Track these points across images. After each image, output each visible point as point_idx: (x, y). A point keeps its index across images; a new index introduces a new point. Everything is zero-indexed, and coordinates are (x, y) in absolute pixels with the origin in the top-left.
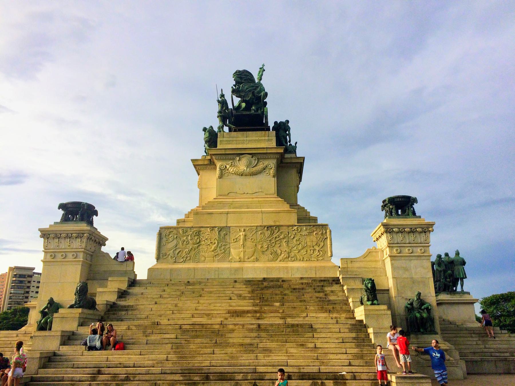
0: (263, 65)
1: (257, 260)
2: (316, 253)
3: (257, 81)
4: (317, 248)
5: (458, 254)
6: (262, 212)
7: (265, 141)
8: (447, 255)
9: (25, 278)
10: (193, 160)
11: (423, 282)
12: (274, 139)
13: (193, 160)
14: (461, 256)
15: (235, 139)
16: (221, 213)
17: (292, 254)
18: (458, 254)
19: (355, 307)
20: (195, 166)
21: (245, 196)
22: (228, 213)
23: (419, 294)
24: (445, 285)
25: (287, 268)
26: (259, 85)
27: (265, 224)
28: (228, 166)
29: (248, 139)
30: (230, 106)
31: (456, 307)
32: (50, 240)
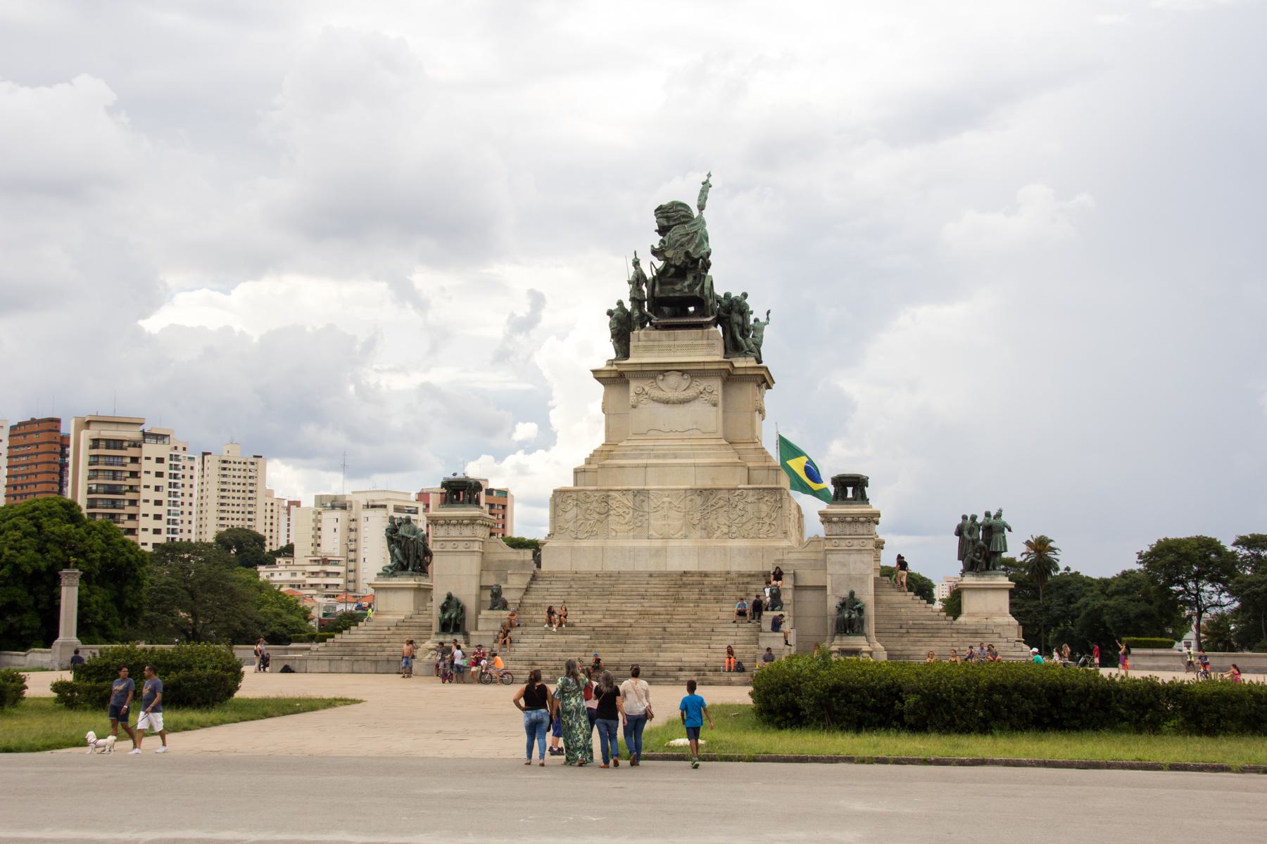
0: (709, 175)
1: (686, 537)
2: (766, 527)
3: (696, 213)
4: (767, 520)
6: (695, 465)
7: (703, 347)
9: (122, 448)
10: (594, 372)
11: (862, 580)
13: (594, 372)
16: (637, 466)
17: (734, 529)
21: (671, 436)
22: (646, 466)
23: (852, 594)
24: (973, 562)
25: (724, 548)
27: (700, 485)
28: (647, 389)
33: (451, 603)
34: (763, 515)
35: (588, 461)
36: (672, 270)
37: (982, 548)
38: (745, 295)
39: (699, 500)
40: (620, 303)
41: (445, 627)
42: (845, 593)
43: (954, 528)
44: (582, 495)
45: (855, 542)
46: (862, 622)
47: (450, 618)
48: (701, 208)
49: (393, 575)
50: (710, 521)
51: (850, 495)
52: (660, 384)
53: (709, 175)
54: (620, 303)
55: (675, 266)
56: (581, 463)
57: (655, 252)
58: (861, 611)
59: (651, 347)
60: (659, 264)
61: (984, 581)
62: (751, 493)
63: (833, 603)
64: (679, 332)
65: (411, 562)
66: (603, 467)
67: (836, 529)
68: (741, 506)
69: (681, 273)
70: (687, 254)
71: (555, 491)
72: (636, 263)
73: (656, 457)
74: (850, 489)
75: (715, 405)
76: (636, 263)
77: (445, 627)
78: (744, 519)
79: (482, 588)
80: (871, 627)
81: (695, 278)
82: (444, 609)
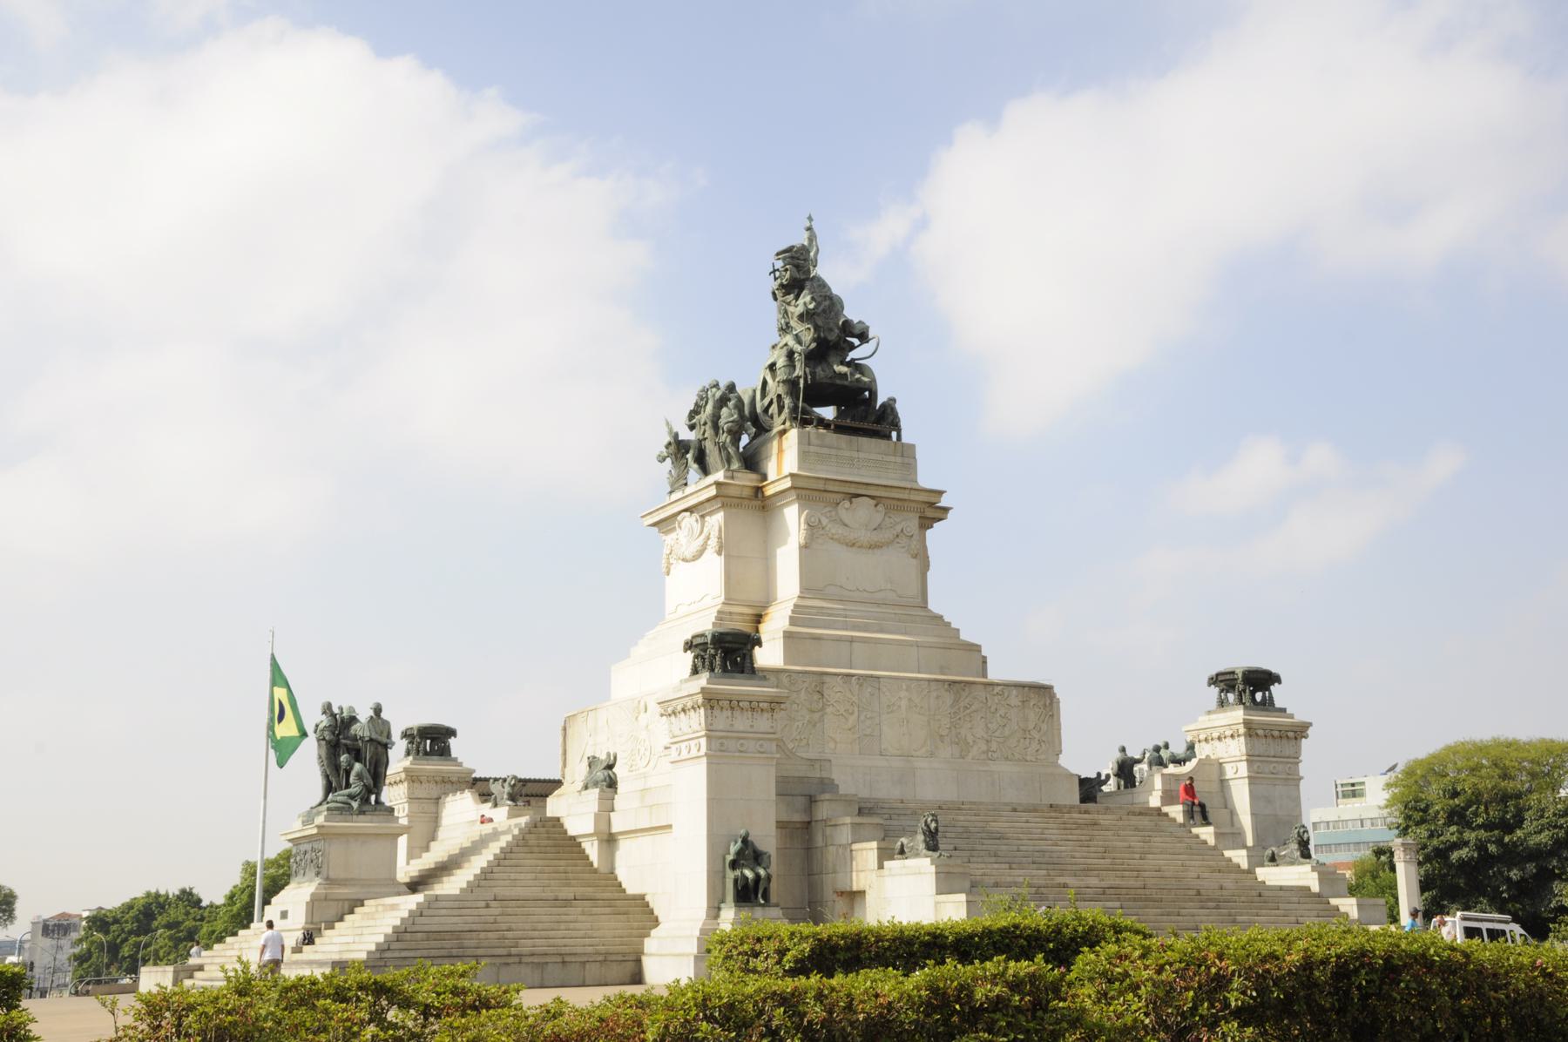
1: (932, 755)
2: (1035, 746)
15: (833, 452)
16: (839, 639)
17: (994, 746)
22: (852, 640)
28: (825, 521)
29: (862, 455)
32: (717, 712)
39: (948, 698)
64: (864, 441)
68: (1002, 712)
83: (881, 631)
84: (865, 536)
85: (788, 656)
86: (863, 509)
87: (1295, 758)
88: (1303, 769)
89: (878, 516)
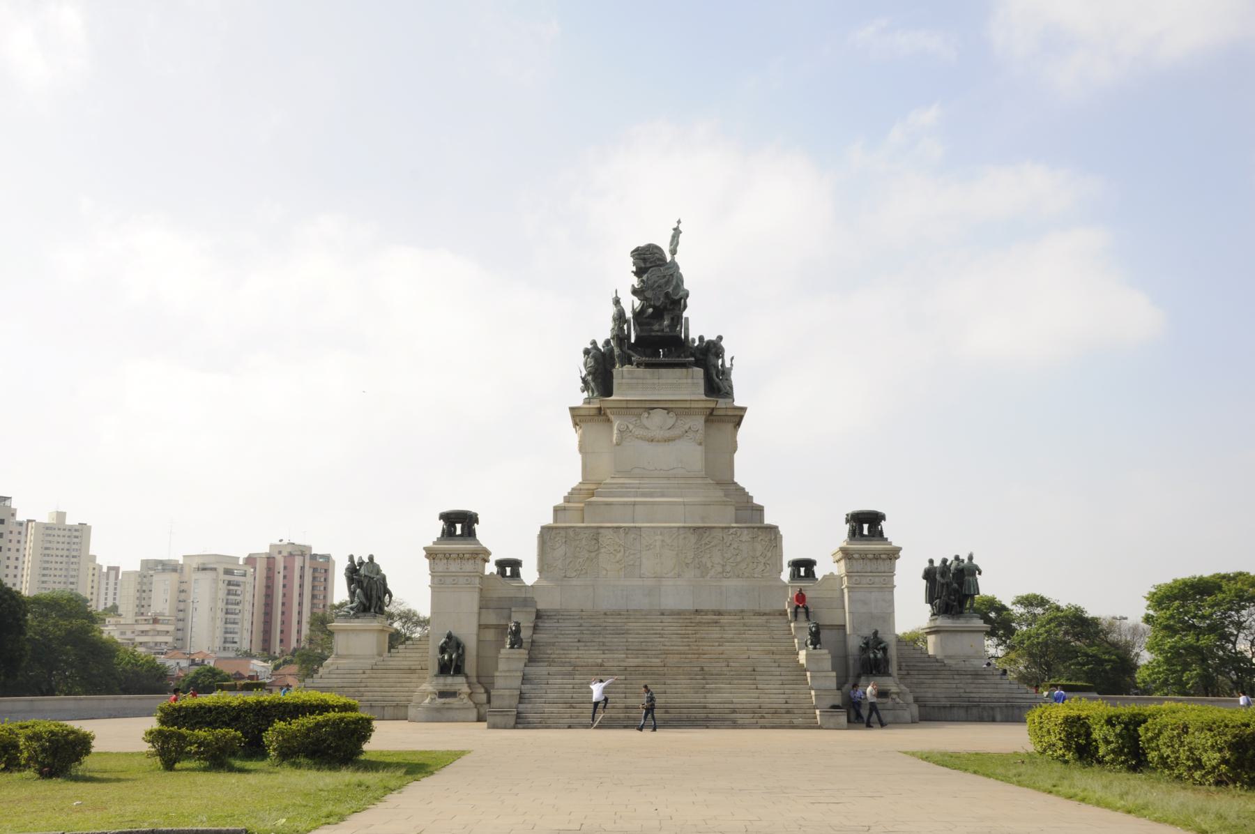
0: (679, 222)
1: (679, 576)
2: (761, 567)
3: (669, 258)
5: (971, 558)
7: (685, 386)
8: (957, 558)
10: (572, 409)
12: (702, 382)
14: (974, 561)
16: (625, 504)
17: (728, 568)
18: (971, 558)
19: (800, 649)
20: (573, 417)
22: (634, 504)
23: (876, 633)
24: (947, 605)
26: (674, 265)
28: (631, 427)
30: (629, 315)
31: (959, 636)
33: (452, 644)
34: (758, 554)
35: (567, 499)
36: (651, 310)
37: (956, 591)
38: (720, 338)
39: (693, 538)
40: (594, 343)
41: (444, 669)
42: (867, 632)
43: (921, 573)
44: (571, 532)
45: (877, 580)
46: (886, 661)
47: (450, 659)
48: (673, 252)
49: (356, 616)
50: (704, 560)
51: (866, 532)
52: (645, 422)
53: (679, 222)
54: (594, 343)
55: (654, 307)
56: (560, 501)
57: (635, 292)
58: (885, 650)
59: (631, 383)
60: (637, 303)
61: (960, 623)
62: (745, 532)
63: (854, 643)
64: (663, 371)
65: (374, 602)
66: (590, 504)
67: (858, 566)
68: (735, 545)
69: (659, 314)
70: (667, 294)
71: (543, 528)
72: (617, 302)
73: (643, 495)
74: (866, 526)
75: (700, 444)
76: (617, 302)
77: (444, 669)
78: (739, 559)
79: (482, 627)
80: (893, 668)
81: (672, 319)
82: (443, 650)
83: (663, 495)
84: (659, 434)
85: (555, 520)
86: (658, 418)
87: (891, 572)
88: (897, 580)
89: (671, 419)
